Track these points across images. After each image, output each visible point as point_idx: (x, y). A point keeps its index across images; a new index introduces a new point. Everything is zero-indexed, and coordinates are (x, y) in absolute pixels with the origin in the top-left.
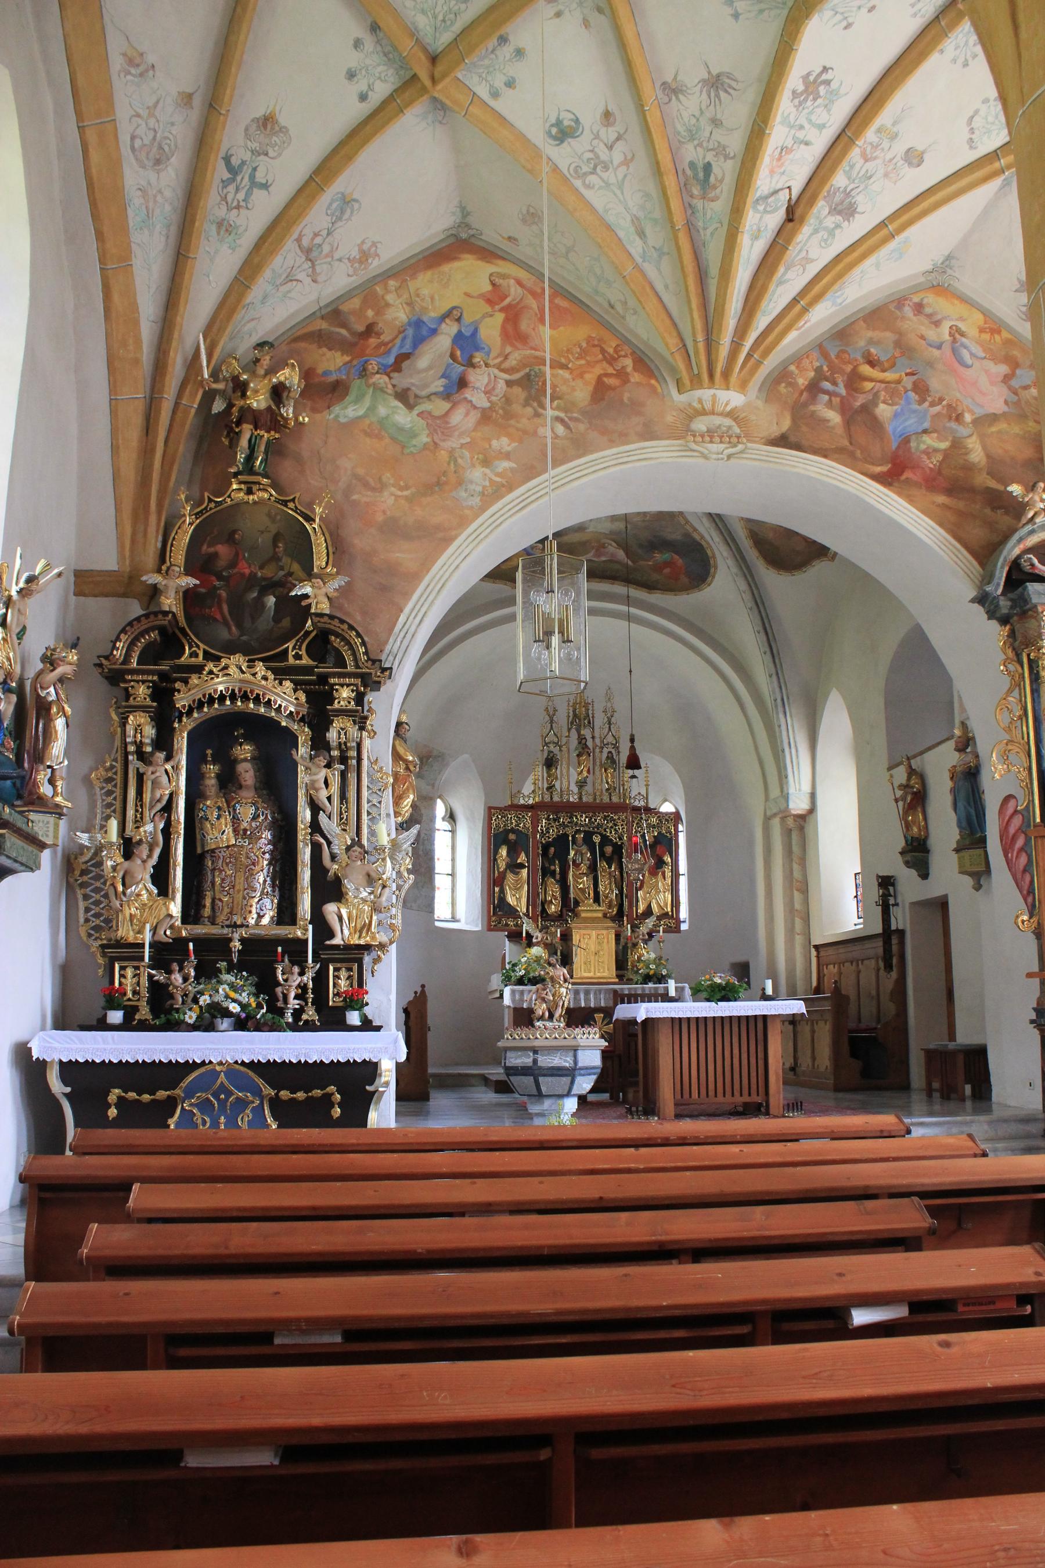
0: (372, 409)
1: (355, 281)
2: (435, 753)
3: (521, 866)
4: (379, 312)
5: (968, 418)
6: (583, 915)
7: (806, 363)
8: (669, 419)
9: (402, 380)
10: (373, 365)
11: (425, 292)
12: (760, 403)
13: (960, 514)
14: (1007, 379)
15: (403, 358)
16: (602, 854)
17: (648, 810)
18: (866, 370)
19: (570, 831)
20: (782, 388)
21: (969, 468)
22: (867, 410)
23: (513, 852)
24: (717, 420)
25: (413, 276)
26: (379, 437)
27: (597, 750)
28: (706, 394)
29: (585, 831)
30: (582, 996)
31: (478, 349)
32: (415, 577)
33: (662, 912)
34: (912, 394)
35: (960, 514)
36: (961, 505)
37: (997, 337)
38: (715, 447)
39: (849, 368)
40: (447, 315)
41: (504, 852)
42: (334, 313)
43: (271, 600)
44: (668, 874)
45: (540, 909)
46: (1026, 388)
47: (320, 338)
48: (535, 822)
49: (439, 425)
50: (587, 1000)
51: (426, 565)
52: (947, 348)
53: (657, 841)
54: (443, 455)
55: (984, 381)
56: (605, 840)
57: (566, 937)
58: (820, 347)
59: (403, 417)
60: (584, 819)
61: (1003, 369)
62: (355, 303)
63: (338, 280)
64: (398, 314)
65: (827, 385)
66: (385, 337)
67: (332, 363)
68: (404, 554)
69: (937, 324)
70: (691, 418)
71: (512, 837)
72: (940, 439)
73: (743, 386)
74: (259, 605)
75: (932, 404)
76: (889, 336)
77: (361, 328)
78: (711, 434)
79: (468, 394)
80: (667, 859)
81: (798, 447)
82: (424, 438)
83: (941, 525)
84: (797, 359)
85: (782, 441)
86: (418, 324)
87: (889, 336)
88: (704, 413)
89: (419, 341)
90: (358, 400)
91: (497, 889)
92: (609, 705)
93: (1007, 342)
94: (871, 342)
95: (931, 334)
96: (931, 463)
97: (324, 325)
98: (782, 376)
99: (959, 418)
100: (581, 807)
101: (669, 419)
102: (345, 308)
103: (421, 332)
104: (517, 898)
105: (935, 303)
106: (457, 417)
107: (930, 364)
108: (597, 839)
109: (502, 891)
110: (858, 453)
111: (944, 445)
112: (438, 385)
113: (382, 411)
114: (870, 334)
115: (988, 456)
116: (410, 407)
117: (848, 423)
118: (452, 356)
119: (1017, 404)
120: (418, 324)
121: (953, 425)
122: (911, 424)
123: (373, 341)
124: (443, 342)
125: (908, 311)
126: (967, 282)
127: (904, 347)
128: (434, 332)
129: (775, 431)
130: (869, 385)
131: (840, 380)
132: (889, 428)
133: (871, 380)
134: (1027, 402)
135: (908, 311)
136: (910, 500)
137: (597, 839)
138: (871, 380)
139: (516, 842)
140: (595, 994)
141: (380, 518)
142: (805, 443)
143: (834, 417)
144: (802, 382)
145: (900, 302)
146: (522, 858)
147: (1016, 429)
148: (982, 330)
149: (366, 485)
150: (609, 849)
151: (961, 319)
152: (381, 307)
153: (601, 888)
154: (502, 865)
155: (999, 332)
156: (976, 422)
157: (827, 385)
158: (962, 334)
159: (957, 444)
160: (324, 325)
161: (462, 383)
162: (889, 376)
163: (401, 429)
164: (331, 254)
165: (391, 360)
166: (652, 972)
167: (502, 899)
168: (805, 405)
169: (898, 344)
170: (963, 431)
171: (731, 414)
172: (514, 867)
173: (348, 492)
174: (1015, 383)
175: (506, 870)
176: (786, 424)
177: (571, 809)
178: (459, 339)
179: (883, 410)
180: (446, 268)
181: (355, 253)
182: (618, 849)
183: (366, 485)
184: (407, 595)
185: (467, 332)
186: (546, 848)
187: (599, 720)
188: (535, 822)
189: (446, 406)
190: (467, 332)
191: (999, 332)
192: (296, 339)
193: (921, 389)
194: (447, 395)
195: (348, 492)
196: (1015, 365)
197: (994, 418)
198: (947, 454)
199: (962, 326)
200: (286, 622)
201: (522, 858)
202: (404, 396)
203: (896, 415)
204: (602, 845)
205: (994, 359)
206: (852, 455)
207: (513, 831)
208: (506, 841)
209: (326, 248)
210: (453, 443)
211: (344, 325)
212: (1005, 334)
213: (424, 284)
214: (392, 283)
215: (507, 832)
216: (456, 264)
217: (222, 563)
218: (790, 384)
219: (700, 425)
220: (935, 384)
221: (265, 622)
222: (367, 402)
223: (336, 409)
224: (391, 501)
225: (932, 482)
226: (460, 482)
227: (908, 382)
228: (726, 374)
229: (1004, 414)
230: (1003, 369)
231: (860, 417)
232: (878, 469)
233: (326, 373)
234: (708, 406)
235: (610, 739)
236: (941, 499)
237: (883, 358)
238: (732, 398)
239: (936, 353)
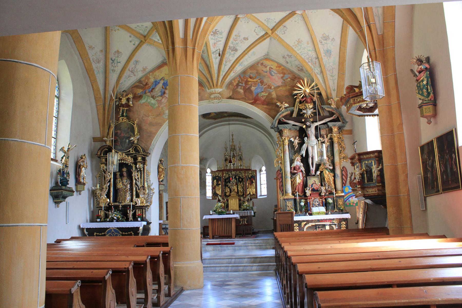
0: (147, 100)
1: (144, 74)
3: (220, 184)
4: (148, 80)
5: (273, 87)
7: (236, 80)
8: (206, 96)
9: (153, 94)
10: (147, 91)
11: (157, 75)
12: (226, 90)
13: (270, 109)
14: (282, 77)
15: (153, 89)
16: (239, 181)
17: (250, 170)
18: (250, 80)
20: (231, 86)
21: (272, 99)
22: (249, 88)
23: (218, 181)
24: (216, 95)
25: (155, 71)
26: (148, 106)
28: (213, 90)
31: (167, 85)
32: (155, 134)
34: (260, 84)
35: (270, 109)
36: (270, 107)
37: (280, 68)
38: (215, 101)
39: (245, 80)
40: (162, 79)
41: (215, 181)
42: (140, 81)
43: (127, 141)
44: (254, 185)
46: (287, 79)
47: (137, 87)
48: (223, 174)
49: (160, 102)
51: (157, 131)
52: (268, 72)
54: (160, 108)
55: (277, 79)
56: (239, 177)
57: (227, 200)
58: (239, 76)
59: (153, 101)
60: (233, 173)
61: (282, 75)
62: (144, 79)
63: (140, 75)
64: (152, 80)
65: (240, 84)
66: (149, 85)
67: (139, 91)
68: (153, 129)
69: (266, 67)
70: (211, 95)
71: (217, 178)
72: (266, 93)
73: (221, 87)
74: (125, 141)
75: (264, 85)
76: (255, 71)
77: (145, 84)
78: (215, 98)
79: (165, 95)
80: (254, 181)
81: (233, 99)
82: (157, 105)
83: (265, 112)
84: (234, 79)
85: (230, 98)
86: (156, 82)
87: (255, 71)
88: (213, 93)
89: (156, 85)
90: (144, 99)
93: (283, 69)
94: (251, 73)
95: (265, 69)
96: (263, 99)
97: (138, 84)
98: (231, 83)
99: (270, 88)
100: (234, 170)
101: (206, 96)
102: (142, 80)
103: (156, 83)
104: (219, 192)
105: (266, 62)
106: (163, 100)
107: (264, 76)
108: (237, 177)
110: (247, 98)
111: (266, 94)
112: (160, 94)
113: (149, 100)
114: (251, 71)
115: (277, 96)
116: (154, 99)
117: (245, 92)
118: (162, 88)
119: (284, 83)
120: (156, 82)
121: (269, 89)
122: (259, 90)
123: (147, 86)
124: (161, 85)
125: (259, 65)
126: (273, 57)
127: (258, 73)
128: (159, 83)
129: (229, 96)
130: (250, 83)
131: (243, 82)
132: (254, 92)
133: (250, 82)
134: (287, 82)
135: (259, 65)
136: (258, 107)
137: (237, 177)
138: (250, 82)
141: (149, 122)
142: (235, 97)
143: (242, 91)
144: (235, 84)
145: (257, 63)
146: (220, 182)
147: (284, 89)
148: (277, 67)
149: (146, 116)
150: (240, 179)
151: (272, 65)
152: (149, 79)
154: (215, 184)
155: (281, 67)
156: (274, 88)
157: (240, 84)
158: (272, 69)
159: (270, 94)
160: (138, 84)
161: (164, 93)
162: (255, 80)
163: (152, 104)
164: (137, 71)
165: (151, 90)
167: (215, 192)
168: (236, 89)
169: (257, 73)
170: (271, 90)
171: (219, 93)
172: (218, 185)
173: (143, 117)
174: (284, 78)
176: (231, 94)
177: (230, 170)
178: (164, 83)
179: (253, 88)
180: (161, 69)
181: (142, 69)
182: (242, 179)
183: (146, 116)
184: (154, 137)
185: (165, 82)
186: (225, 180)
187: (237, 149)
188: (223, 174)
189: (161, 98)
190: (165, 82)
191: (281, 67)
192: (133, 88)
193: (262, 82)
194: (161, 96)
195: (143, 117)
196: (284, 74)
197: (279, 87)
198: (267, 96)
199: (272, 67)
200: (130, 145)
202: (153, 97)
203: (256, 89)
204: (239, 178)
205: (280, 73)
206: (245, 99)
207: (217, 176)
208: (216, 179)
209: (135, 70)
210: (162, 106)
211: (142, 84)
212: (282, 67)
213: (157, 73)
214: (151, 74)
215: (216, 177)
216: (163, 68)
217: (119, 134)
218: (232, 85)
219: (212, 96)
220: (265, 81)
221: (126, 145)
222: (146, 99)
223: (140, 101)
224: (150, 119)
225: (263, 103)
226: (164, 114)
227: (259, 81)
228: (217, 85)
229: (281, 86)
230: (282, 75)
231: (248, 90)
232: (251, 101)
233: (138, 94)
234: (214, 92)
235: (240, 153)
236: (265, 106)
237: (253, 76)
238: (219, 90)
239: (266, 74)
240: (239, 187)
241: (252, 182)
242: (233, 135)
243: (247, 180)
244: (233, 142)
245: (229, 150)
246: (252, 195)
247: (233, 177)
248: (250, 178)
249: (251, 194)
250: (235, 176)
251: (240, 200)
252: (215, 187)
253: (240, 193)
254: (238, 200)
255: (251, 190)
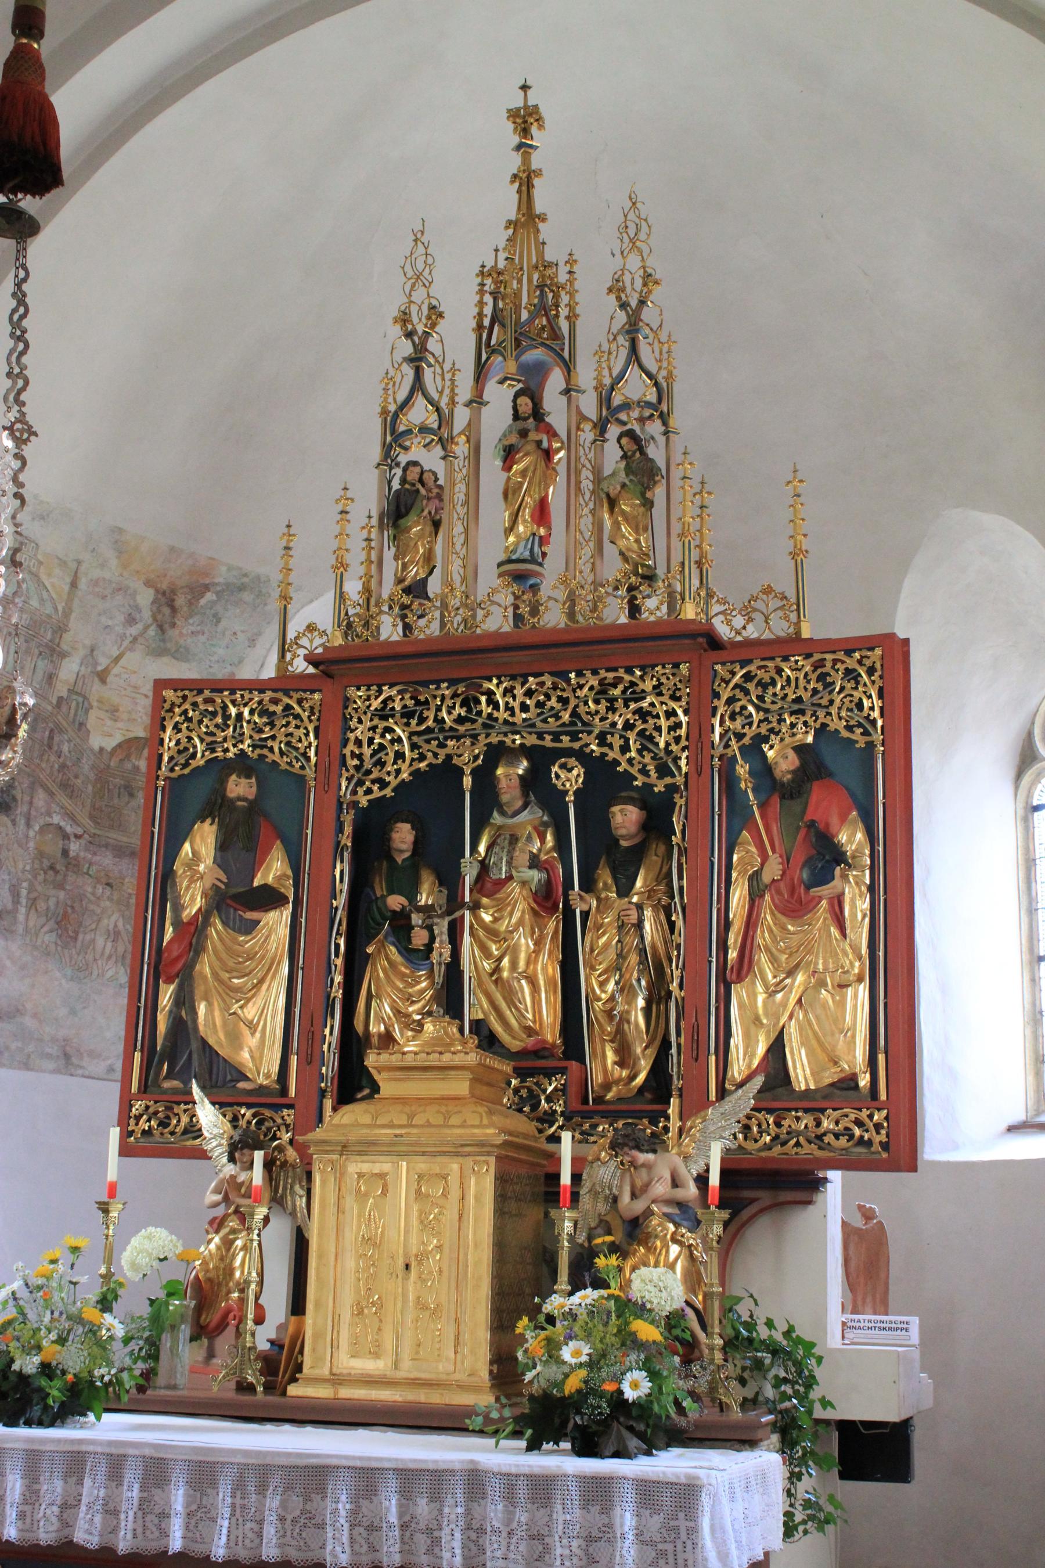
2: (222, 576)
3: (269, 898)
6: (387, 1088)
19: (468, 756)
27: (588, 435)
29: (525, 751)
30: (178, 1498)
33: (830, 1076)
41: (202, 844)
44: (857, 906)
45: (330, 1068)
48: (335, 724)
50: (199, 1515)
53: (812, 764)
56: (605, 782)
71: (239, 788)
80: (851, 838)
91: (167, 994)
92: (634, 262)
100: (527, 653)
108: (569, 778)
109: (184, 1000)
137: (569, 778)
139: (254, 808)
140: (239, 1487)
146: (274, 870)
150: (625, 818)
153: (588, 980)
166: (573, 1384)
172: (241, 900)
175: (205, 914)
177: (465, 661)
188: (335, 724)
201: (274, 870)
207: (243, 765)
208: (215, 806)
240: (601, 942)
241: (828, 858)
242: (525, 120)
243: (737, 816)
244: (527, 219)
245: (456, 342)
246: (814, 1103)
247: (510, 774)
248: (791, 792)
249: (802, 1073)
250: (541, 760)
251: (529, 1187)
252: (193, 934)
253: (603, 1062)
254: (482, 1186)
255: (793, 1011)
